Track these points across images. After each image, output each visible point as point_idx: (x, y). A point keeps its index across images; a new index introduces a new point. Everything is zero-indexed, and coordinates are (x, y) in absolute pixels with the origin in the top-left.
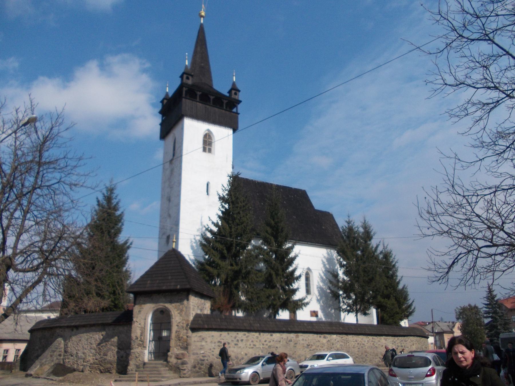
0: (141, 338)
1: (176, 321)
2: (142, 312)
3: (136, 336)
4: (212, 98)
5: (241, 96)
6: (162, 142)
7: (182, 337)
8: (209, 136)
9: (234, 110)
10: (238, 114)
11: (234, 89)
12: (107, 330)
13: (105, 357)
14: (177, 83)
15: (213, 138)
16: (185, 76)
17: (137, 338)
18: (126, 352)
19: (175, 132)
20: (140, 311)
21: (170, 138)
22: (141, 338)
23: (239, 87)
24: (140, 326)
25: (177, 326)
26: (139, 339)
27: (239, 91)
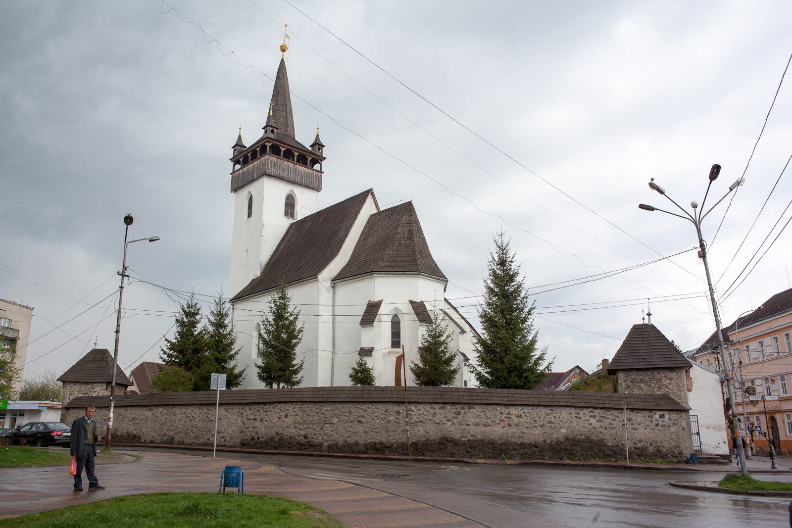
4: (296, 154)
5: (325, 152)
6: (233, 194)
8: (292, 196)
9: (317, 167)
10: (321, 172)
11: (318, 144)
14: (260, 134)
15: (295, 201)
16: (270, 129)
19: (253, 188)
21: (244, 193)
23: (323, 142)
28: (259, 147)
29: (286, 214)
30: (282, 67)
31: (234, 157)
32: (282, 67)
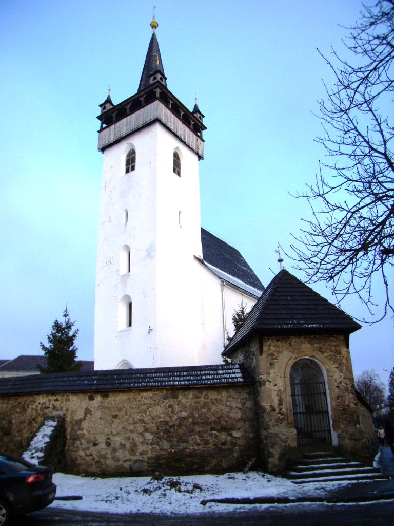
0: (280, 409)
1: (336, 381)
2: (277, 365)
3: (271, 406)
7: (348, 406)
12: (180, 397)
13: (182, 445)
17: (274, 410)
18: (231, 435)
20: (271, 364)
22: (280, 409)
24: (275, 388)
25: (338, 387)
26: (277, 411)
27: (203, 116)
28: (143, 95)
29: (174, 171)
30: (153, 42)
31: (102, 115)
32: (153, 42)
